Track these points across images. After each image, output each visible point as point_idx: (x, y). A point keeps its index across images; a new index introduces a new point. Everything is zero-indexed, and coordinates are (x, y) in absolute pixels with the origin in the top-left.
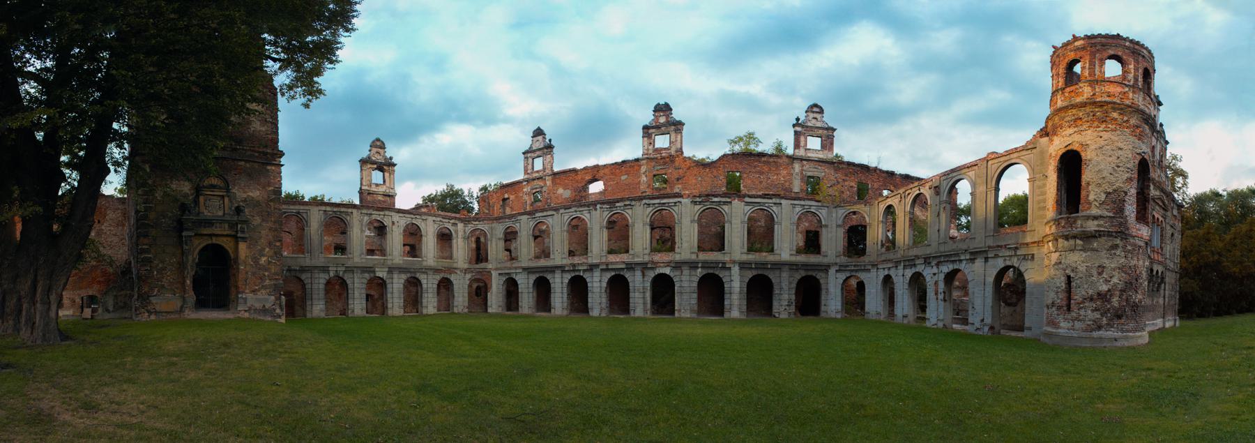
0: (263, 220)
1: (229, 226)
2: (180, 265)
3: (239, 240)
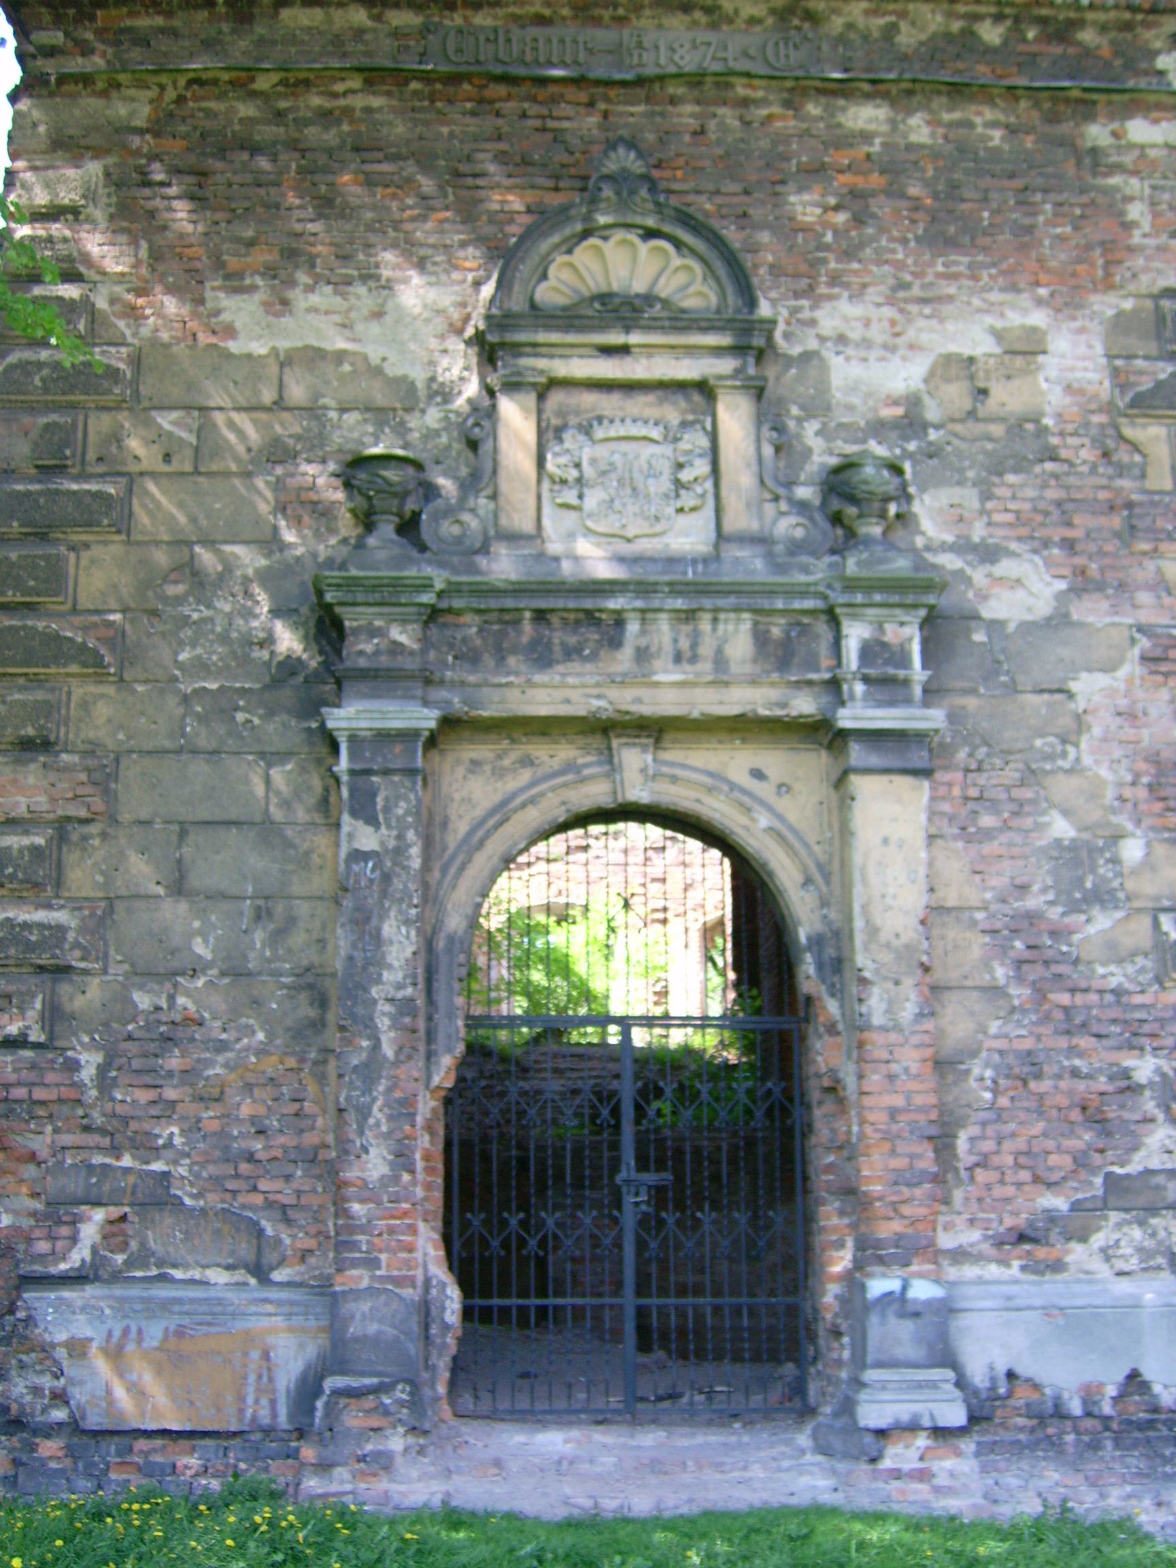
0: (1083, 583)
1: (761, 638)
2: (322, 1002)
3: (856, 753)
